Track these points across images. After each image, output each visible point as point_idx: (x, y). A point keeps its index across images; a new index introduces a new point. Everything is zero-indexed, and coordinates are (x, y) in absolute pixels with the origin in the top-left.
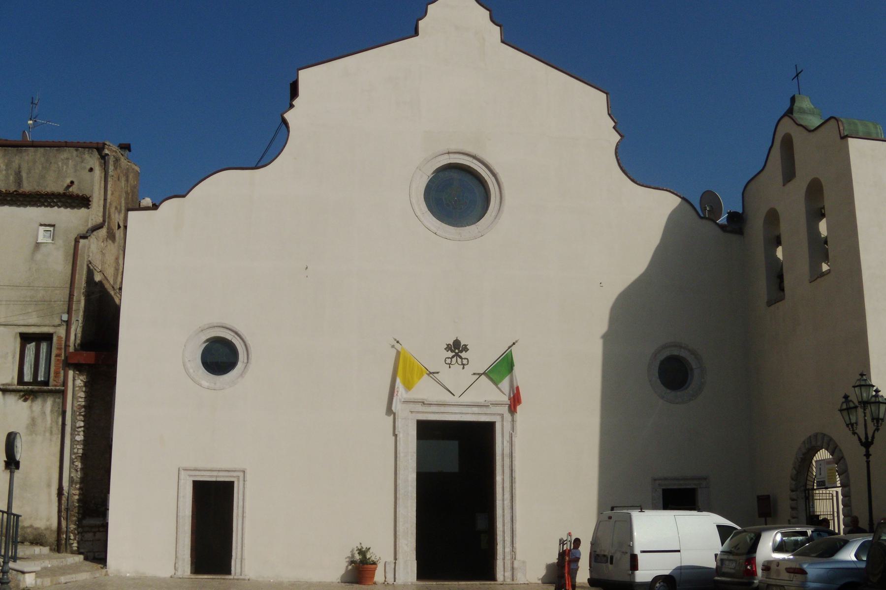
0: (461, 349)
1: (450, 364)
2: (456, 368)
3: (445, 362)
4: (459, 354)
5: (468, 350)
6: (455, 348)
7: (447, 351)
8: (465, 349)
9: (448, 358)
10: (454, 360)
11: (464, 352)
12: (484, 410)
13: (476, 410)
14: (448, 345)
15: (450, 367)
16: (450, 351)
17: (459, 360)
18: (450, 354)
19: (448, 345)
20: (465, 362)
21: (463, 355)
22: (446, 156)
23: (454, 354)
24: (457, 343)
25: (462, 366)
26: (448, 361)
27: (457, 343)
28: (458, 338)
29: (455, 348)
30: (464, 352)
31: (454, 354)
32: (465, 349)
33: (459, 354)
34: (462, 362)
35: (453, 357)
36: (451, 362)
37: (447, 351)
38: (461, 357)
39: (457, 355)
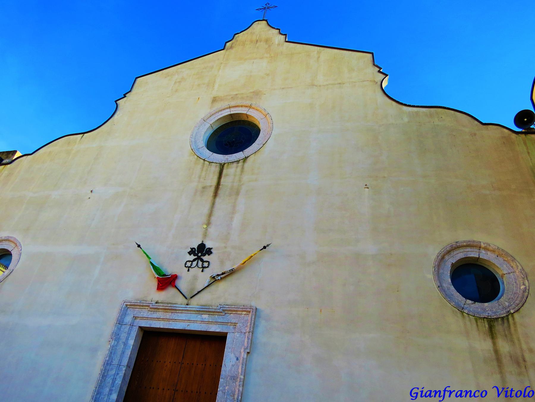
0: (204, 252)
1: (190, 267)
2: (196, 271)
3: (185, 265)
4: (202, 257)
5: (211, 253)
6: (198, 252)
7: (190, 255)
8: (209, 252)
9: (189, 261)
10: (195, 263)
11: (207, 255)
12: (216, 318)
13: (205, 317)
14: (192, 249)
15: (188, 271)
16: (192, 255)
17: (200, 263)
18: (192, 257)
19: (192, 249)
20: (206, 264)
21: (205, 258)
22: (228, 110)
23: (196, 257)
24: (202, 246)
25: (202, 269)
26: (189, 264)
27: (202, 246)
28: (204, 243)
29: (198, 252)
30: (207, 255)
31: (196, 257)
32: (209, 252)
33: (202, 257)
34: (203, 264)
35: (194, 260)
36: (191, 266)
37: (190, 255)
38: (203, 261)
39: (199, 258)
